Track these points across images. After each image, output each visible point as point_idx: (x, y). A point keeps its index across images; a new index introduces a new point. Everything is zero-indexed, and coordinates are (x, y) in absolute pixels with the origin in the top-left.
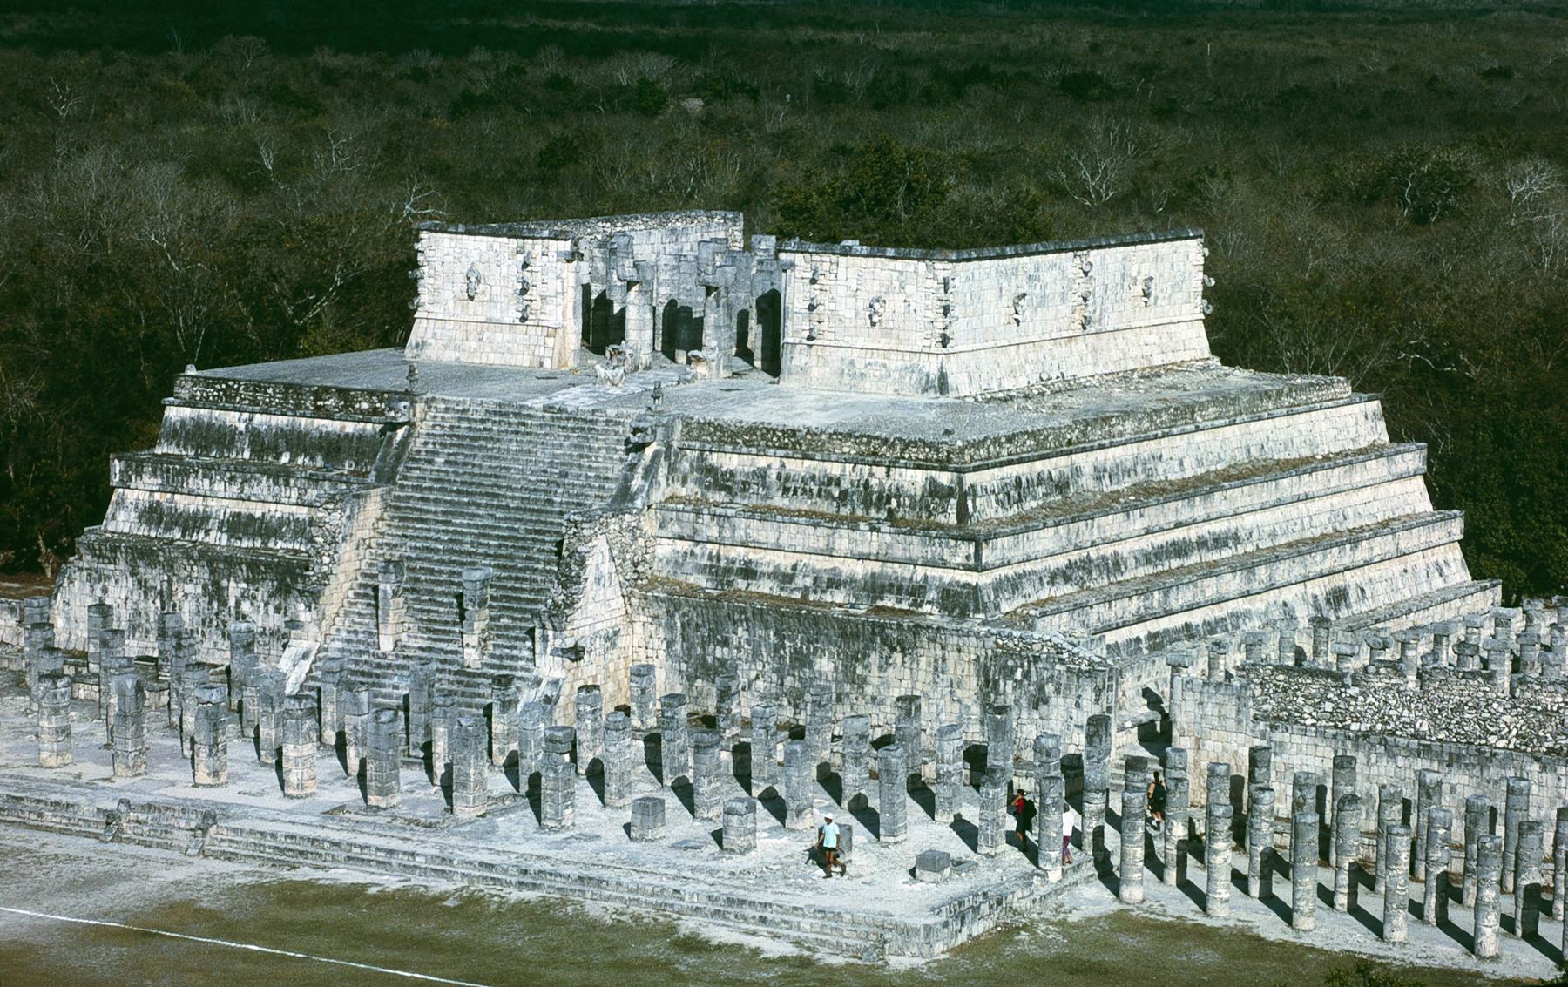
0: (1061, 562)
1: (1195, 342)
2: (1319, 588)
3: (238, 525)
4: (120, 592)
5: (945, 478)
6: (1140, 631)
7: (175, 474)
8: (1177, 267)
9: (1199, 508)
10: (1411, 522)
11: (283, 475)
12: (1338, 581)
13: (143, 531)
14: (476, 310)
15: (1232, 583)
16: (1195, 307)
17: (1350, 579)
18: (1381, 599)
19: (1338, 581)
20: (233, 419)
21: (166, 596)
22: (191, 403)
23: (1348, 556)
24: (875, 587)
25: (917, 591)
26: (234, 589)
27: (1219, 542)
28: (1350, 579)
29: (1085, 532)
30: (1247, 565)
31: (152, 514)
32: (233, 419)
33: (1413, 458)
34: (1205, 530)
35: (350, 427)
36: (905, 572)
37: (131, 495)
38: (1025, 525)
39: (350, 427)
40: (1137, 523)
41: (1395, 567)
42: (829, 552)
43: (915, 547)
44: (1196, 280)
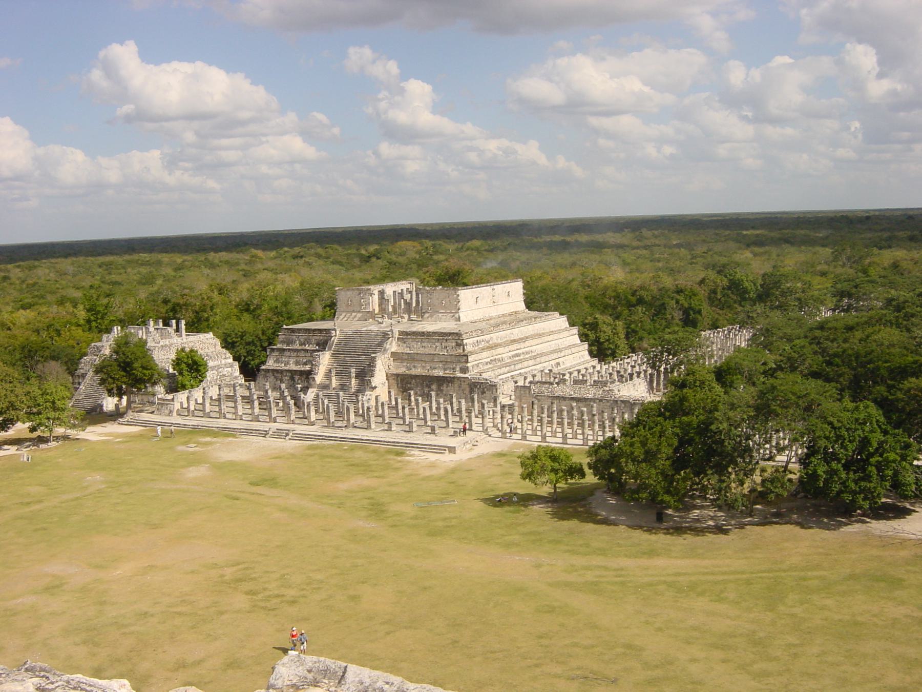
0: (489, 360)
1: (522, 306)
2: (553, 363)
6: (509, 375)
8: (516, 288)
9: (522, 345)
10: (574, 346)
12: (557, 361)
15: (531, 362)
16: (522, 298)
17: (560, 360)
18: (568, 365)
19: (557, 361)
23: (560, 355)
26: (297, 377)
27: (527, 353)
28: (560, 360)
29: (494, 352)
30: (534, 358)
33: (575, 330)
34: (524, 350)
40: (507, 349)
41: (571, 357)
44: (521, 291)
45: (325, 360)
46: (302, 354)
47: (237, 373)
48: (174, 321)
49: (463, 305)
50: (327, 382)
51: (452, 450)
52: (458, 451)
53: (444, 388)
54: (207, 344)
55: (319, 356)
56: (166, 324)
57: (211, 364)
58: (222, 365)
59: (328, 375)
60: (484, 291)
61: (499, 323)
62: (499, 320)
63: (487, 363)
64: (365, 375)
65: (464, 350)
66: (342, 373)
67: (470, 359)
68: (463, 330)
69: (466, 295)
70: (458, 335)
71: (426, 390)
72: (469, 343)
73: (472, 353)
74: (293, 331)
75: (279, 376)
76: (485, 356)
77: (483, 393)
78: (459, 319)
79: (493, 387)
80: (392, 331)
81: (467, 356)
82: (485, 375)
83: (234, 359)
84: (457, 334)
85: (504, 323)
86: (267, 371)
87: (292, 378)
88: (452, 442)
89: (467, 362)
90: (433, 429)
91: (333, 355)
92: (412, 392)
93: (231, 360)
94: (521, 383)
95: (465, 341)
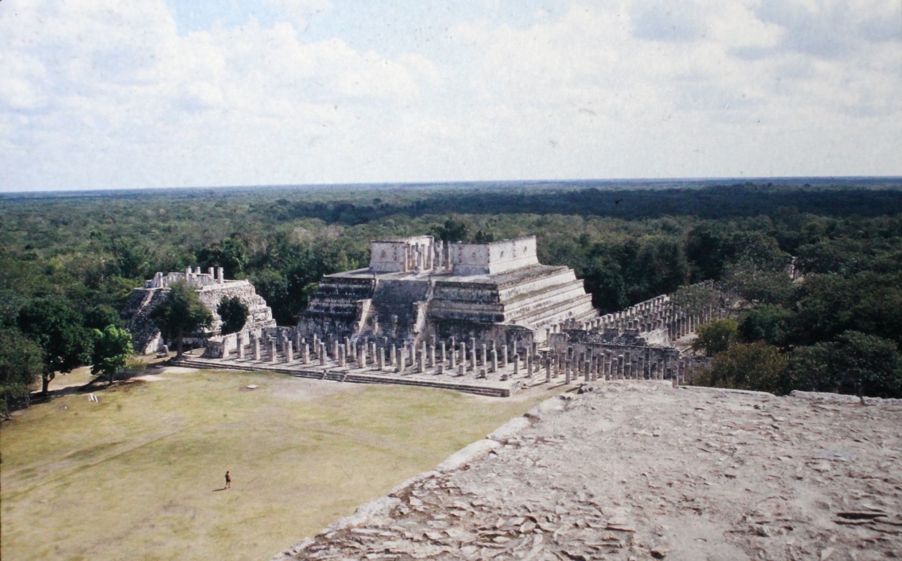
0: (518, 309)
3: (337, 309)
4: (312, 325)
5: (494, 292)
7: (322, 298)
11: (346, 298)
13: (316, 311)
14: (384, 260)
20: (334, 286)
21: (322, 325)
22: (324, 282)
24: (481, 316)
25: (490, 317)
26: (337, 323)
31: (317, 307)
32: (334, 286)
35: (361, 286)
36: (487, 313)
37: (312, 303)
38: (511, 301)
39: (361, 286)
42: (470, 309)
43: (490, 307)
45: (367, 305)
46: (342, 300)
47: (270, 318)
48: (212, 269)
49: (492, 258)
50: (369, 328)
51: (504, 393)
52: (511, 394)
53: (482, 334)
54: (242, 289)
55: (361, 303)
56: (205, 270)
57: (251, 309)
58: (260, 312)
59: (369, 321)
60: (508, 246)
61: (527, 274)
62: (521, 273)
63: (518, 312)
64: (406, 324)
65: (499, 300)
66: (384, 320)
67: (505, 308)
68: (498, 281)
69: (494, 249)
70: (494, 287)
71: (464, 336)
72: (503, 294)
73: (506, 302)
74: (332, 280)
75: (320, 320)
76: (516, 306)
77: (519, 339)
78: (488, 272)
79: (529, 333)
80: (430, 281)
81: (503, 305)
82: (517, 324)
83: (268, 305)
84: (492, 285)
85: (528, 276)
86: (309, 315)
87: (333, 324)
88: (504, 385)
89: (503, 310)
90: (483, 372)
91: (373, 303)
92: (453, 338)
93: (264, 306)
94: (551, 331)
95: (500, 292)
